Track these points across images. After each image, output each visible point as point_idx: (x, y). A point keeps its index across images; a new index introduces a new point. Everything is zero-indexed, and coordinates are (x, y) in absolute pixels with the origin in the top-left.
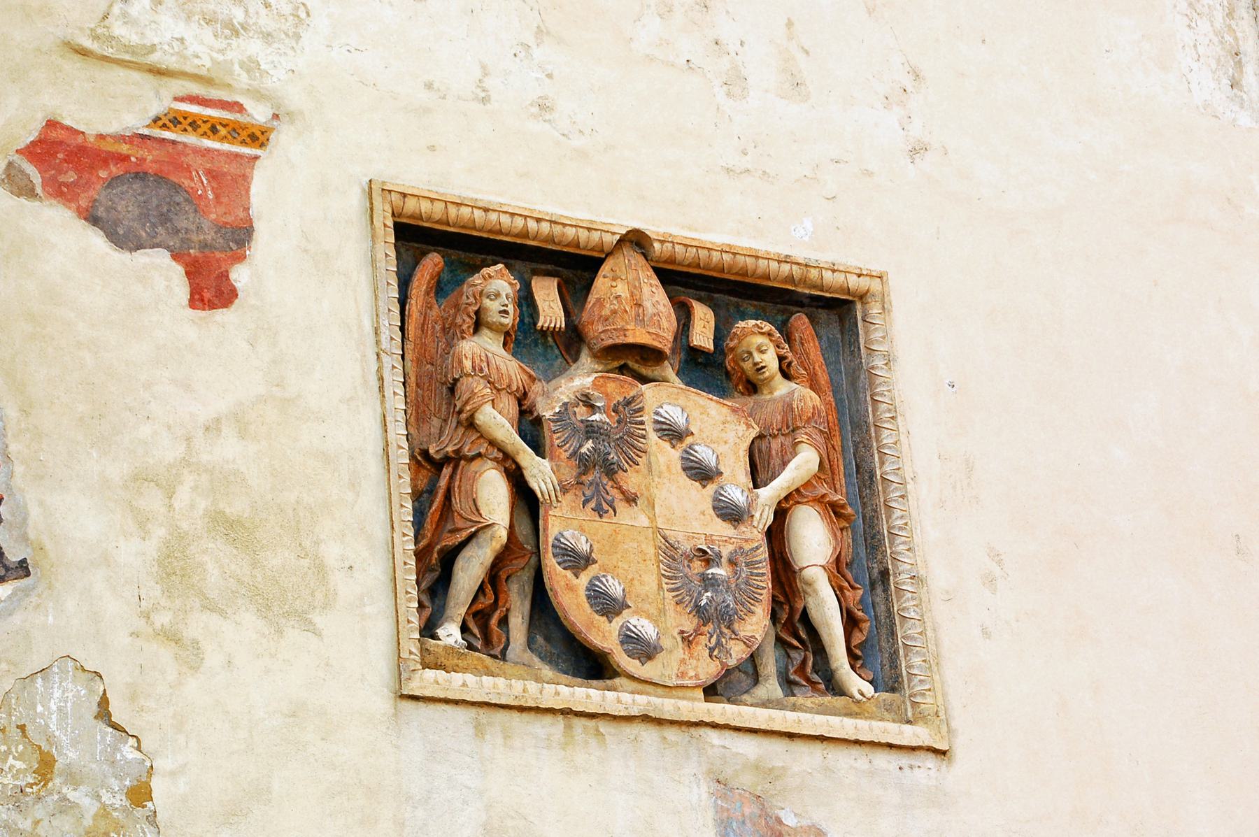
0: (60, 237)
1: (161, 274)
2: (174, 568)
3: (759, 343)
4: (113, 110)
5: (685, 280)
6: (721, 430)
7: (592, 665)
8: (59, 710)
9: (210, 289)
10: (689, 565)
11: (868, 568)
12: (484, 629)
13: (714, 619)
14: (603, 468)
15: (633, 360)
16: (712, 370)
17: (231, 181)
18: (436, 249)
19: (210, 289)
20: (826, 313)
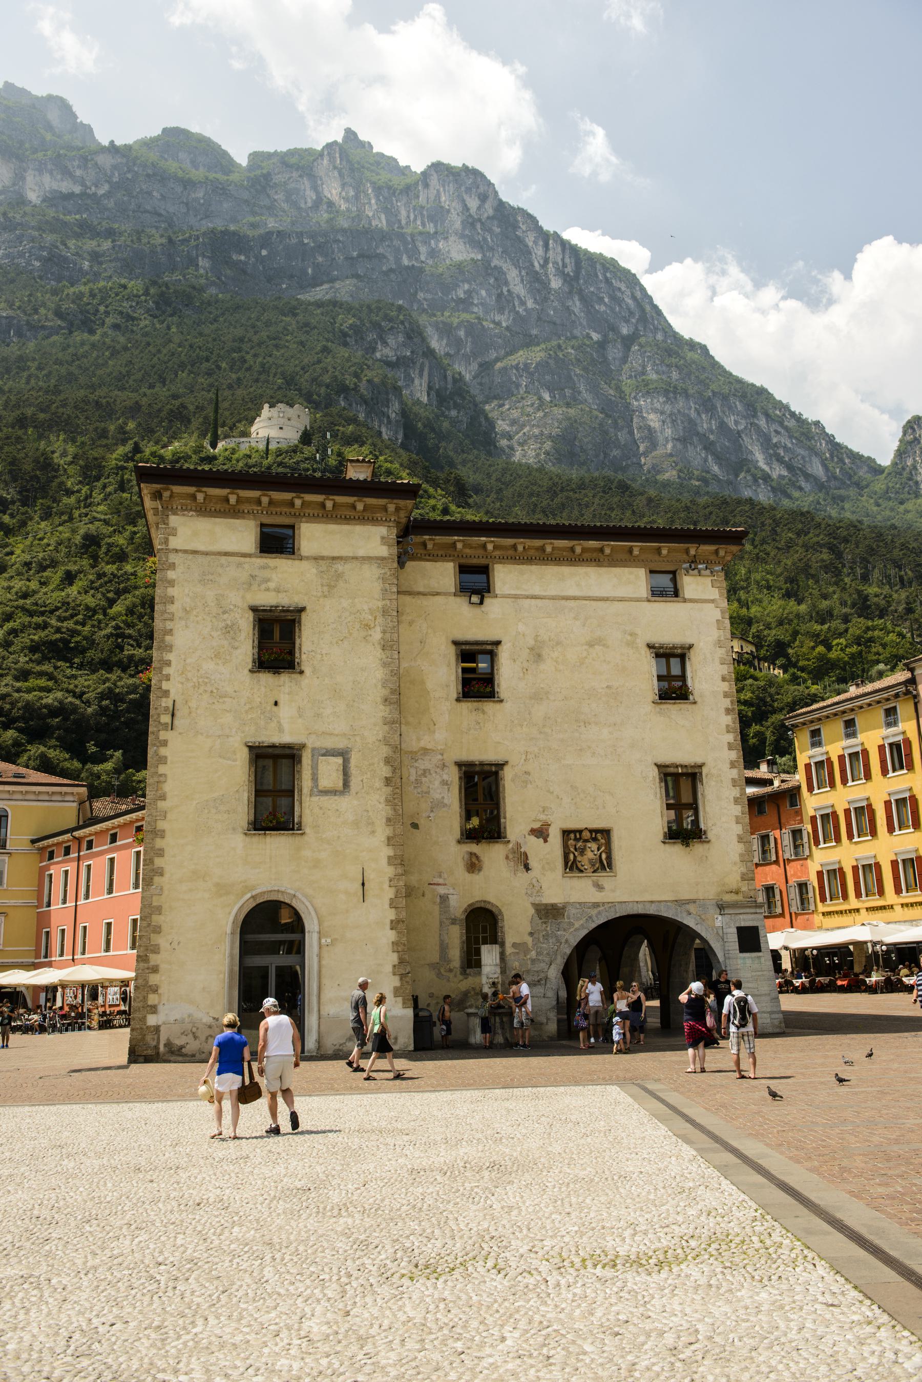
0: (533, 839)
1: (541, 840)
2: (543, 868)
3: (599, 836)
4: (537, 825)
5: (591, 831)
6: (594, 846)
7: (581, 871)
8: (534, 881)
9: (546, 841)
10: (590, 861)
11: (609, 858)
12: (571, 869)
13: (593, 865)
14: (582, 852)
15: (586, 841)
16: (595, 839)
17: (547, 830)
18: (566, 833)
19: (546, 841)
20: (606, 833)
